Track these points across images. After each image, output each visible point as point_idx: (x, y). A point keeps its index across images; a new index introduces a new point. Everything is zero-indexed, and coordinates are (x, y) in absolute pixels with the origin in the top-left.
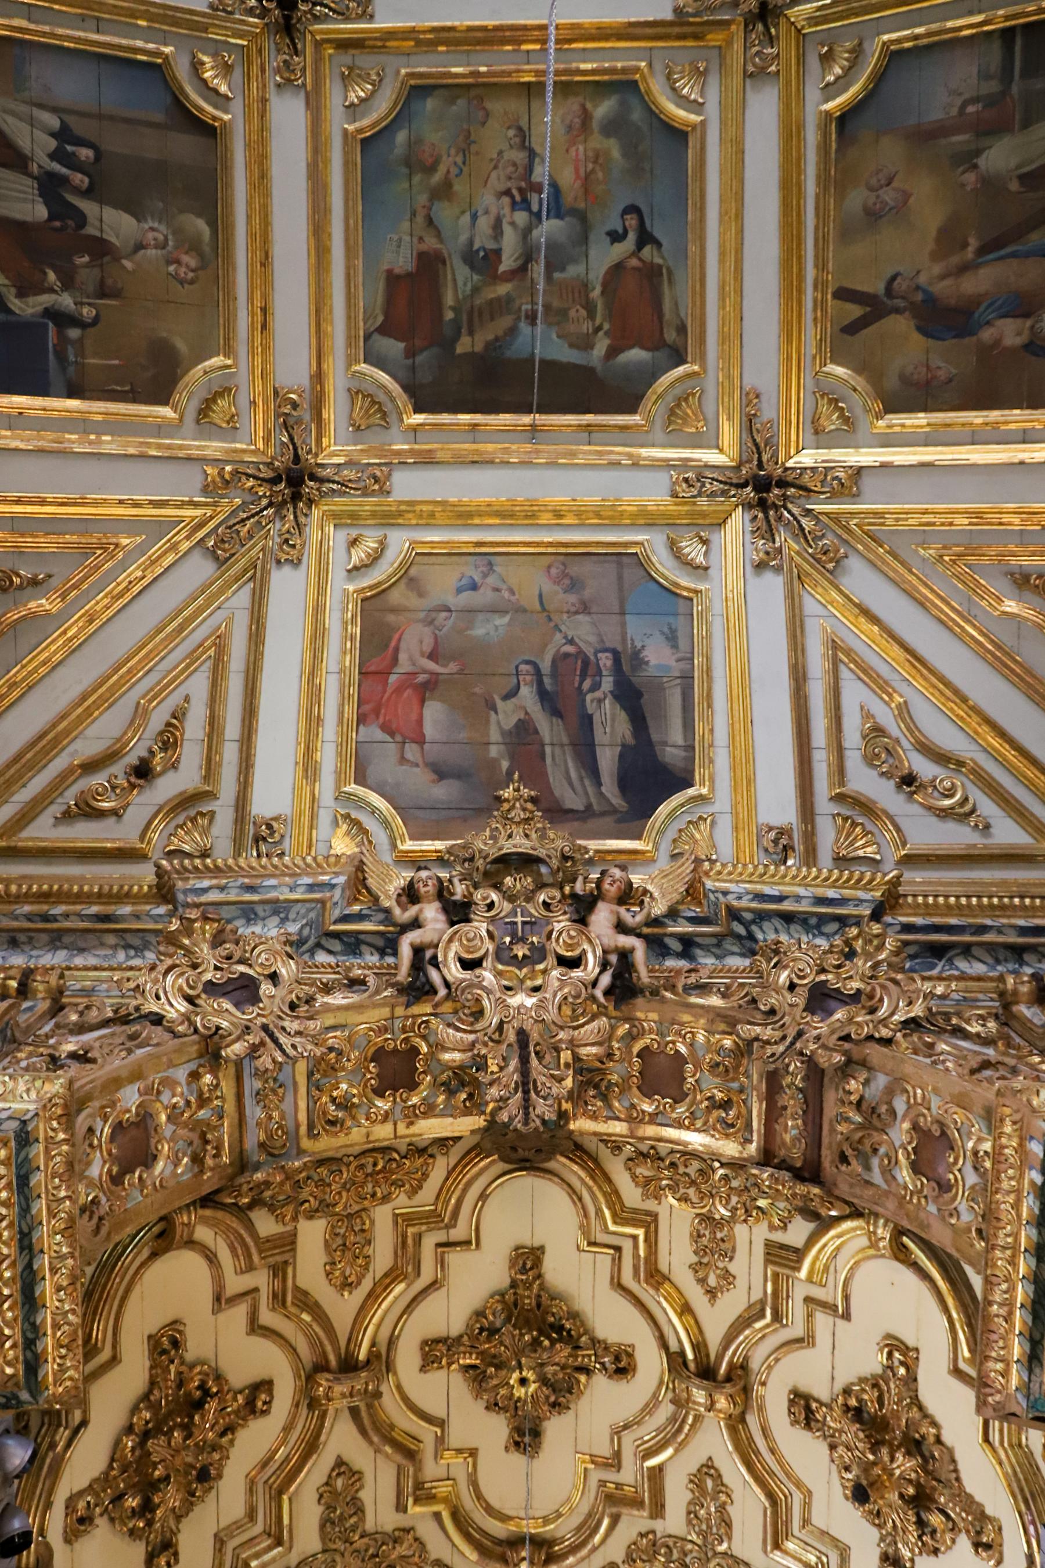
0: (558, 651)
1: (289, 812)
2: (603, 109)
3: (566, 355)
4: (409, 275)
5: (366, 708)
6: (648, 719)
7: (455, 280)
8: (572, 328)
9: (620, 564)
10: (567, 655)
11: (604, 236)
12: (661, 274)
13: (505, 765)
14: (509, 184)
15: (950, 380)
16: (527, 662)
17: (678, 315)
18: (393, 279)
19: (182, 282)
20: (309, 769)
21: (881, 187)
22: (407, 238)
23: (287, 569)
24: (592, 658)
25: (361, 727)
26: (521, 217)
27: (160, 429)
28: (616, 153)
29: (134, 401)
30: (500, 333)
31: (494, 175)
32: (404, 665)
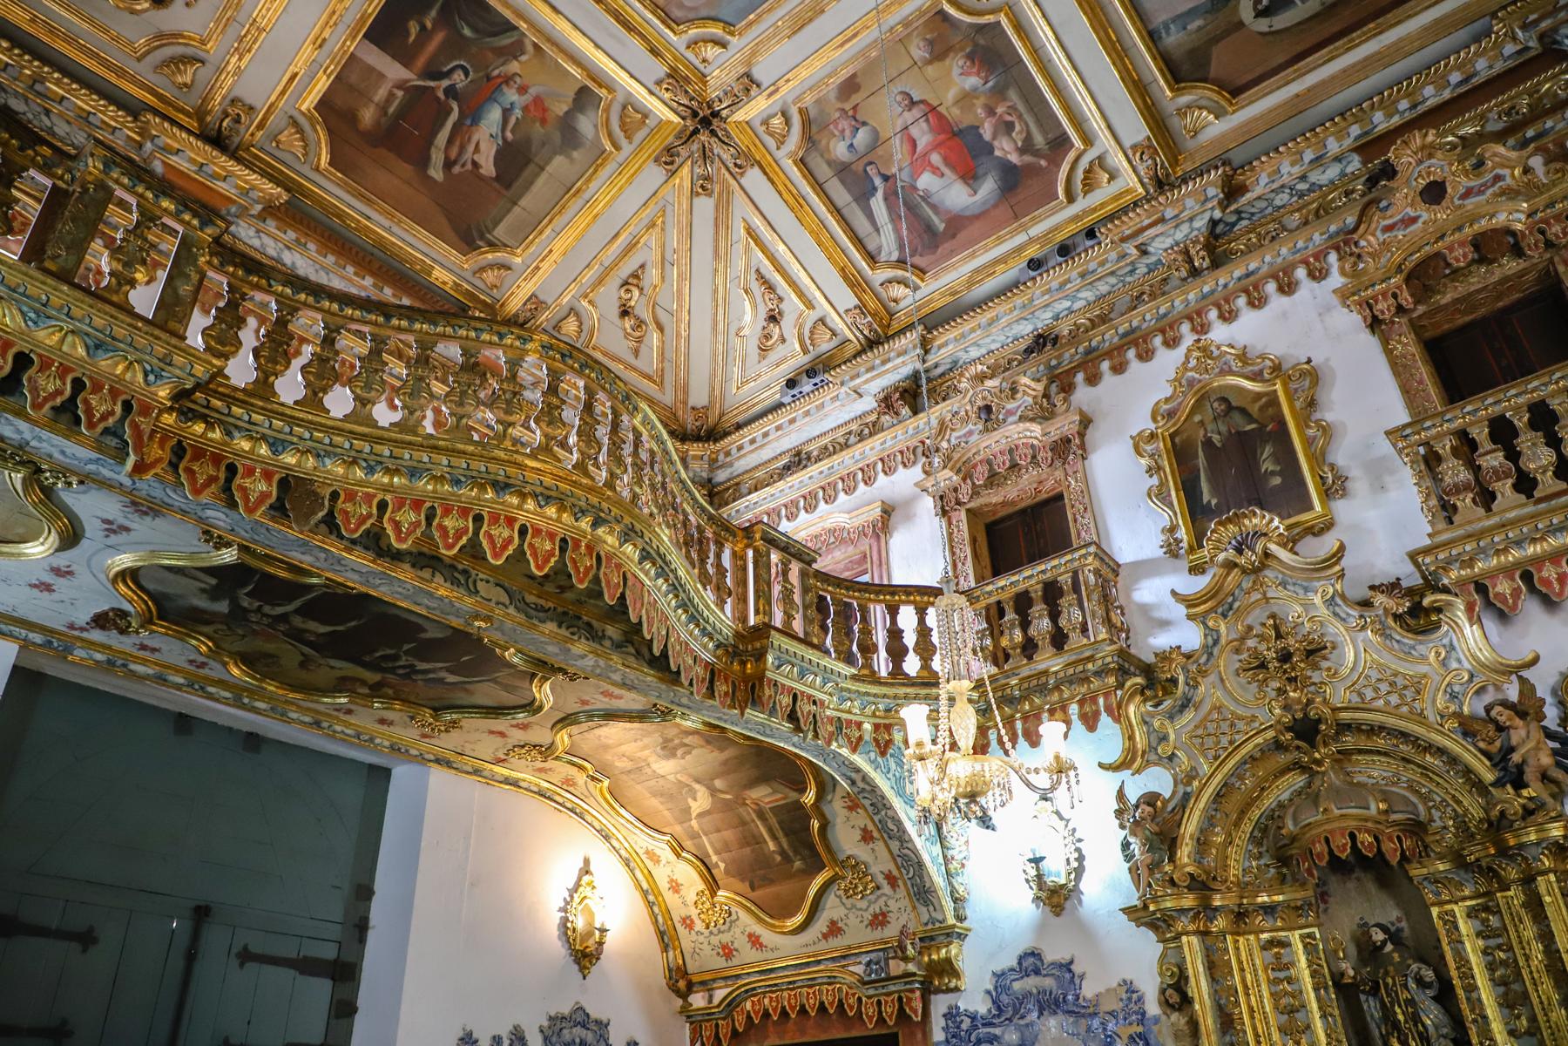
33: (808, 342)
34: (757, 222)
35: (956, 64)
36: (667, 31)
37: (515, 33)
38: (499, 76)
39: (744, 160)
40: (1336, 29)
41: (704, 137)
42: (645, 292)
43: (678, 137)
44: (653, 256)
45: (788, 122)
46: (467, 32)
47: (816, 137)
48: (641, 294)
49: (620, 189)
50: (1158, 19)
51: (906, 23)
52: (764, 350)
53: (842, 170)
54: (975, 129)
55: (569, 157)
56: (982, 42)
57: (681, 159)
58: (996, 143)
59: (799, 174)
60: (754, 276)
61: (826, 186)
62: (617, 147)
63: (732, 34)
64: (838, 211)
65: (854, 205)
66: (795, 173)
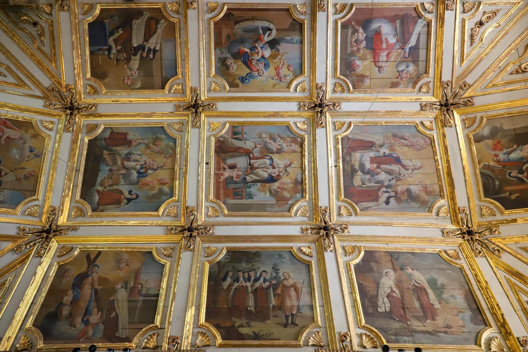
2: (166, 189)
3: (99, 179)
4: (126, 138)
7: (123, 150)
8: (106, 180)
14: (148, 164)
15: (61, 282)
18: (126, 134)
19: (123, 80)
22: (136, 138)
26: (138, 167)
27: (84, 74)
28: (153, 192)
30: (107, 162)
31: (151, 160)
32: (6, 130)
33: (476, 6)
34: (457, 62)
35: (359, 71)
36: (435, 138)
37: (482, 171)
38: (500, 165)
39: (444, 85)
40: (253, 12)
41: (451, 101)
42: (520, 64)
43: (459, 107)
44: (503, 74)
45: (421, 88)
46: (497, 183)
47: (416, 77)
48: (522, 64)
49: (494, 105)
50: (297, 46)
51: (365, 92)
52: (495, 13)
53: (415, 61)
54: (366, 47)
55: (501, 126)
56: (348, 72)
57: (464, 99)
58: (363, 39)
59: (430, 69)
60: (474, 44)
61: (425, 59)
62: (482, 118)
63: (417, 124)
64: (427, 49)
65: (421, 47)
66: (431, 71)
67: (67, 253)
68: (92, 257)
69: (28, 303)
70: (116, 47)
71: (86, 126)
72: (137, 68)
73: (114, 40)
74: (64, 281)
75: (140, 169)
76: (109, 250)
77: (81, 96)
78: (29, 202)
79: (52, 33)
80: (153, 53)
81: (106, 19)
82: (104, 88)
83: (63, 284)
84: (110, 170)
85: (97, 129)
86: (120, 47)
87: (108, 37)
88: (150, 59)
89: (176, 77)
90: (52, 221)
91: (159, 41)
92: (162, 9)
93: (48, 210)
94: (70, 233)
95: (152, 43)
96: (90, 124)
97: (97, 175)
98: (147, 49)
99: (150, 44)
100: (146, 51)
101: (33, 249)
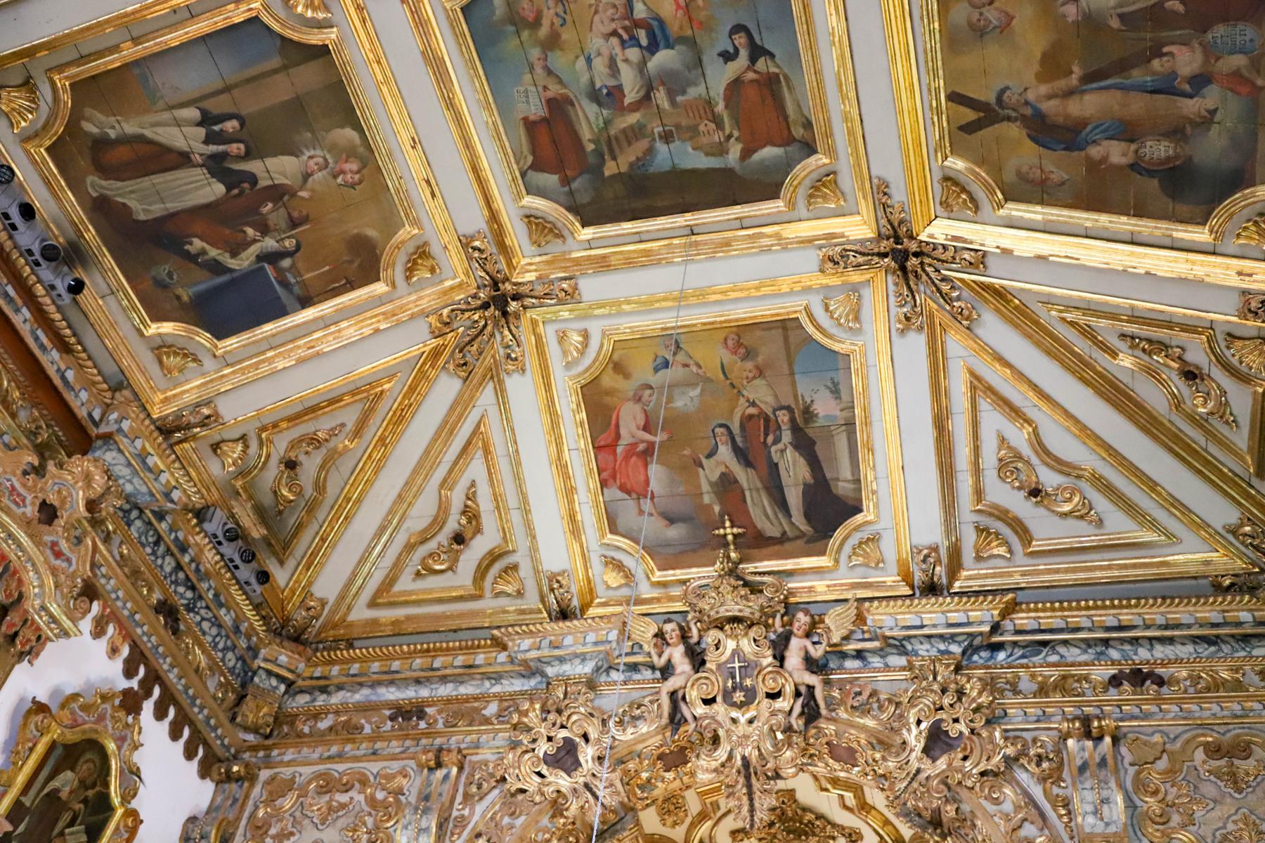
0: (743, 413)
1: (566, 566)
4: (544, 120)
5: (605, 475)
6: (823, 465)
7: (587, 118)
8: (704, 140)
9: (785, 329)
10: (751, 417)
11: (716, 56)
12: (779, 82)
13: (717, 509)
14: (613, 26)
15: (1063, 183)
16: (721, 426)
17: (803, 115)
19: (353, 186)
20: (575, 528)
21: (984, 5)
22: (533, 89)
23: (516, 376)
24: (772, 416)
25: (605, 490)
26: (633, 54)
29: (353, 289)
30: (640, 155)
31: (597, 18)
32: (625, 440)
67: (964, 190)
68: (970, 115)
69: (1132, 253)
70: (255, 241)
71: (539, 246)
72: (293, 159)
73: (234, 254)
74: (1057, 175)
75: (640, 46)
76: (941, 72)
77: (452, 288)
78: (818, 327)
79: (294, 419)
80: (215, 124)
81: (178, 298)
82: (402, 234)
83: (1067, 177)
84: (667, 137)
85: (539, 214)
86: (250, 231)
87: (235, 275)
88: (242, 125)
89: (267, 19)
90: (866, 254)
91: (166, 116)
92: (48, 143)
93: (833, 274)
94: (898, 195)
95: (188, 138)
96: (530, 238)
97: (694, 172)
98: (213, 148)
99: (191, 143)
100: (221, 148)
101: (961, 280)
